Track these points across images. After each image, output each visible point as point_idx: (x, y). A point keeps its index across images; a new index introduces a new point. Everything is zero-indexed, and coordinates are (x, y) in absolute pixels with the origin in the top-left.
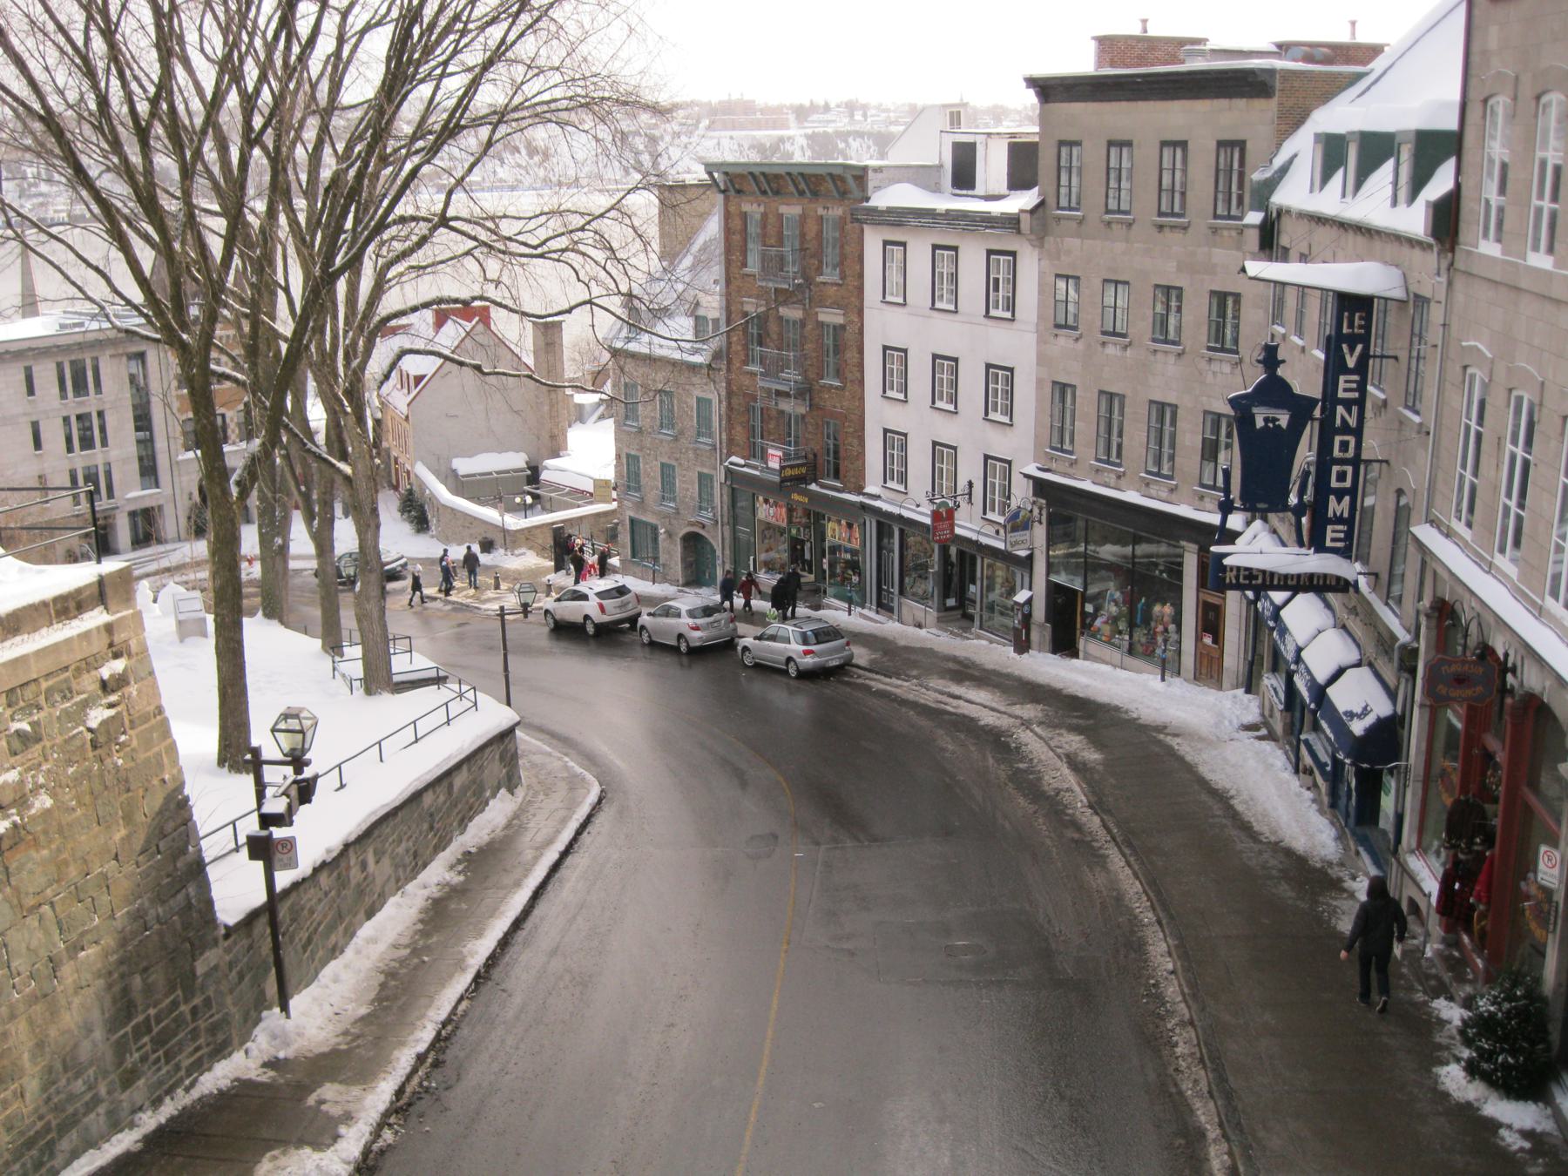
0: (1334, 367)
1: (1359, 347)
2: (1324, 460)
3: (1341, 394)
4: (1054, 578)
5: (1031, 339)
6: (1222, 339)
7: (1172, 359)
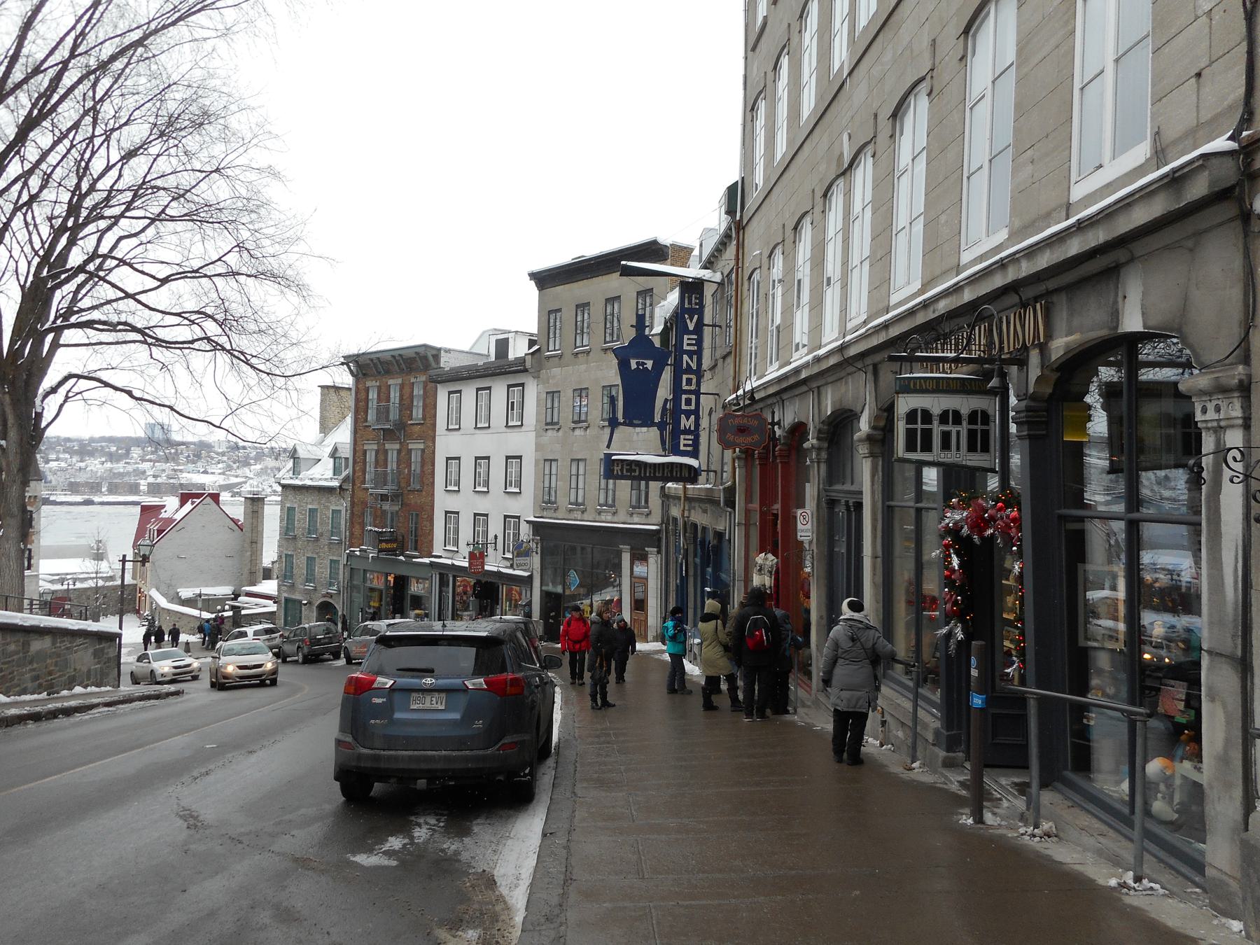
2: (677, 389)
3: (685, 347)
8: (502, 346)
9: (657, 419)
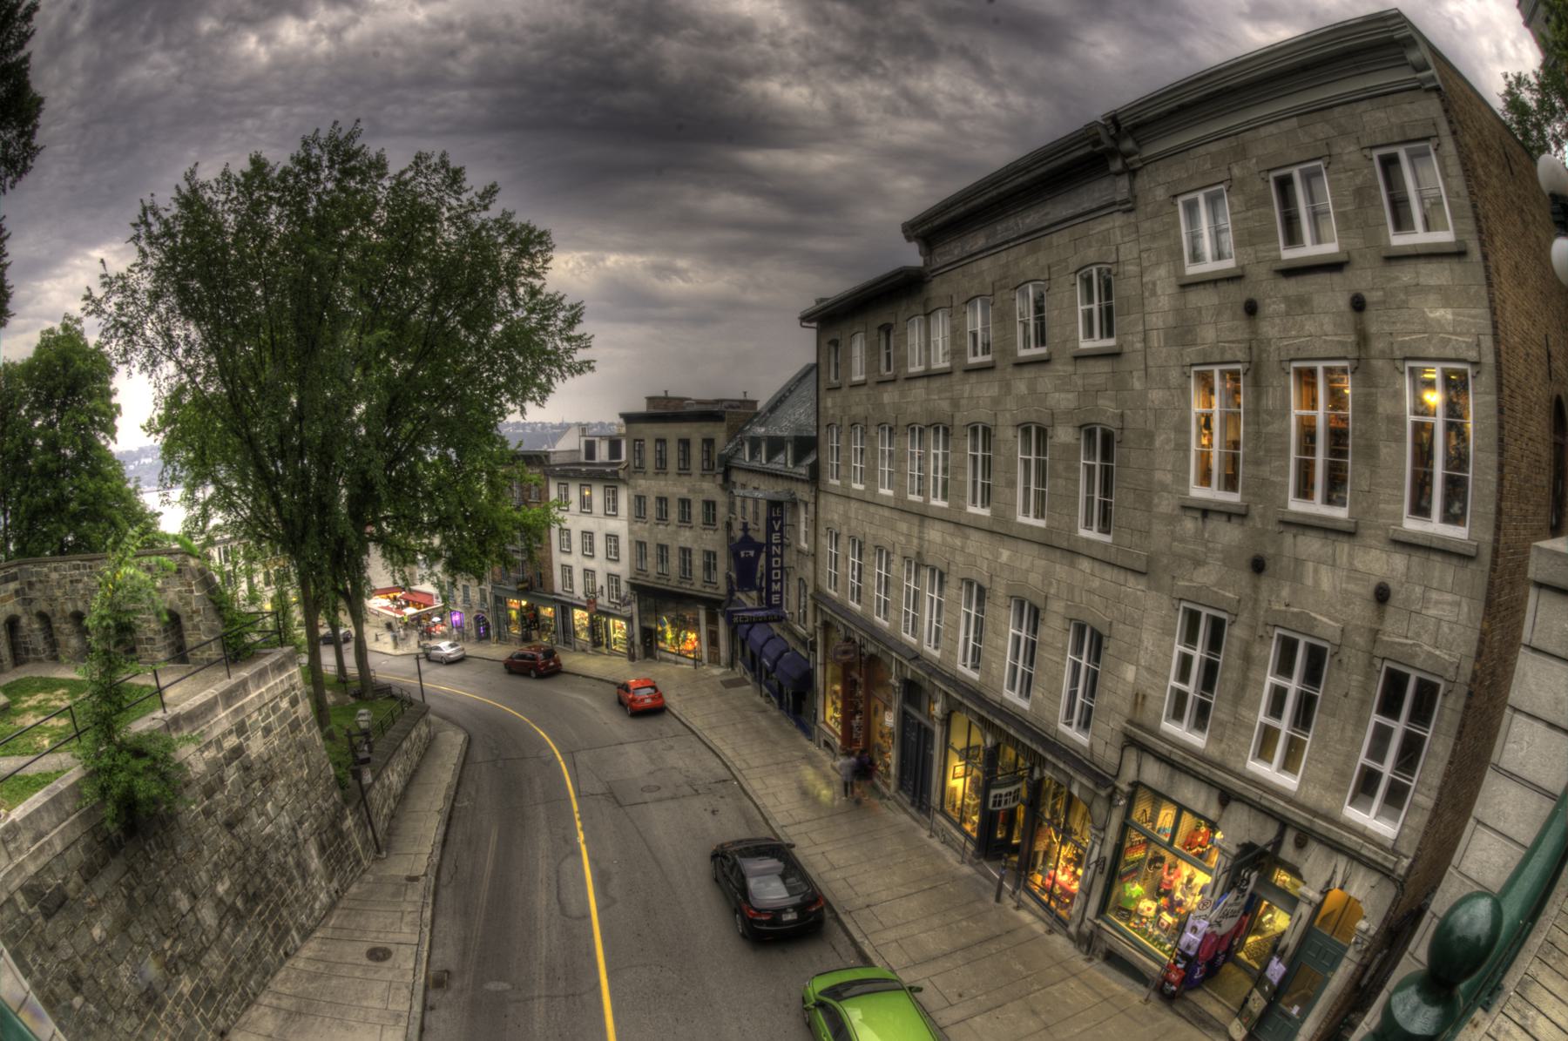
0: (770, 530)
2: (769, 568)
4: (646, 624)
5: (625, 523)
8: (590, 449)
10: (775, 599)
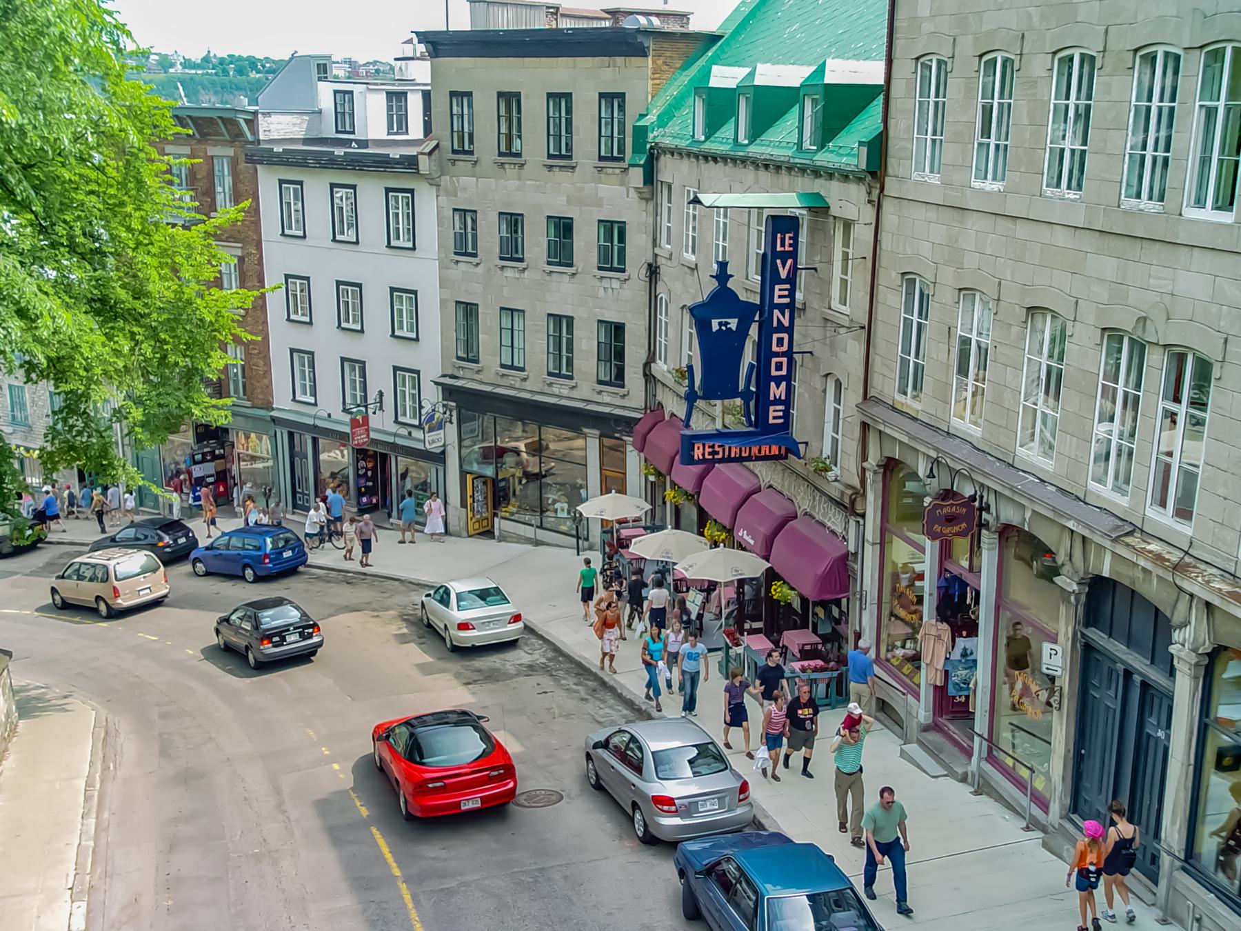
0: (769, 275)
1: (789, 262)
2: (764, 352)
3: (777, 300)
6: (612, 258)
7: (566, 278)
9: (741, 387)
10: (775, 413)
